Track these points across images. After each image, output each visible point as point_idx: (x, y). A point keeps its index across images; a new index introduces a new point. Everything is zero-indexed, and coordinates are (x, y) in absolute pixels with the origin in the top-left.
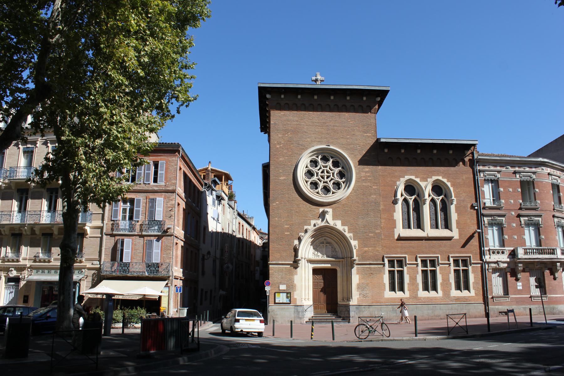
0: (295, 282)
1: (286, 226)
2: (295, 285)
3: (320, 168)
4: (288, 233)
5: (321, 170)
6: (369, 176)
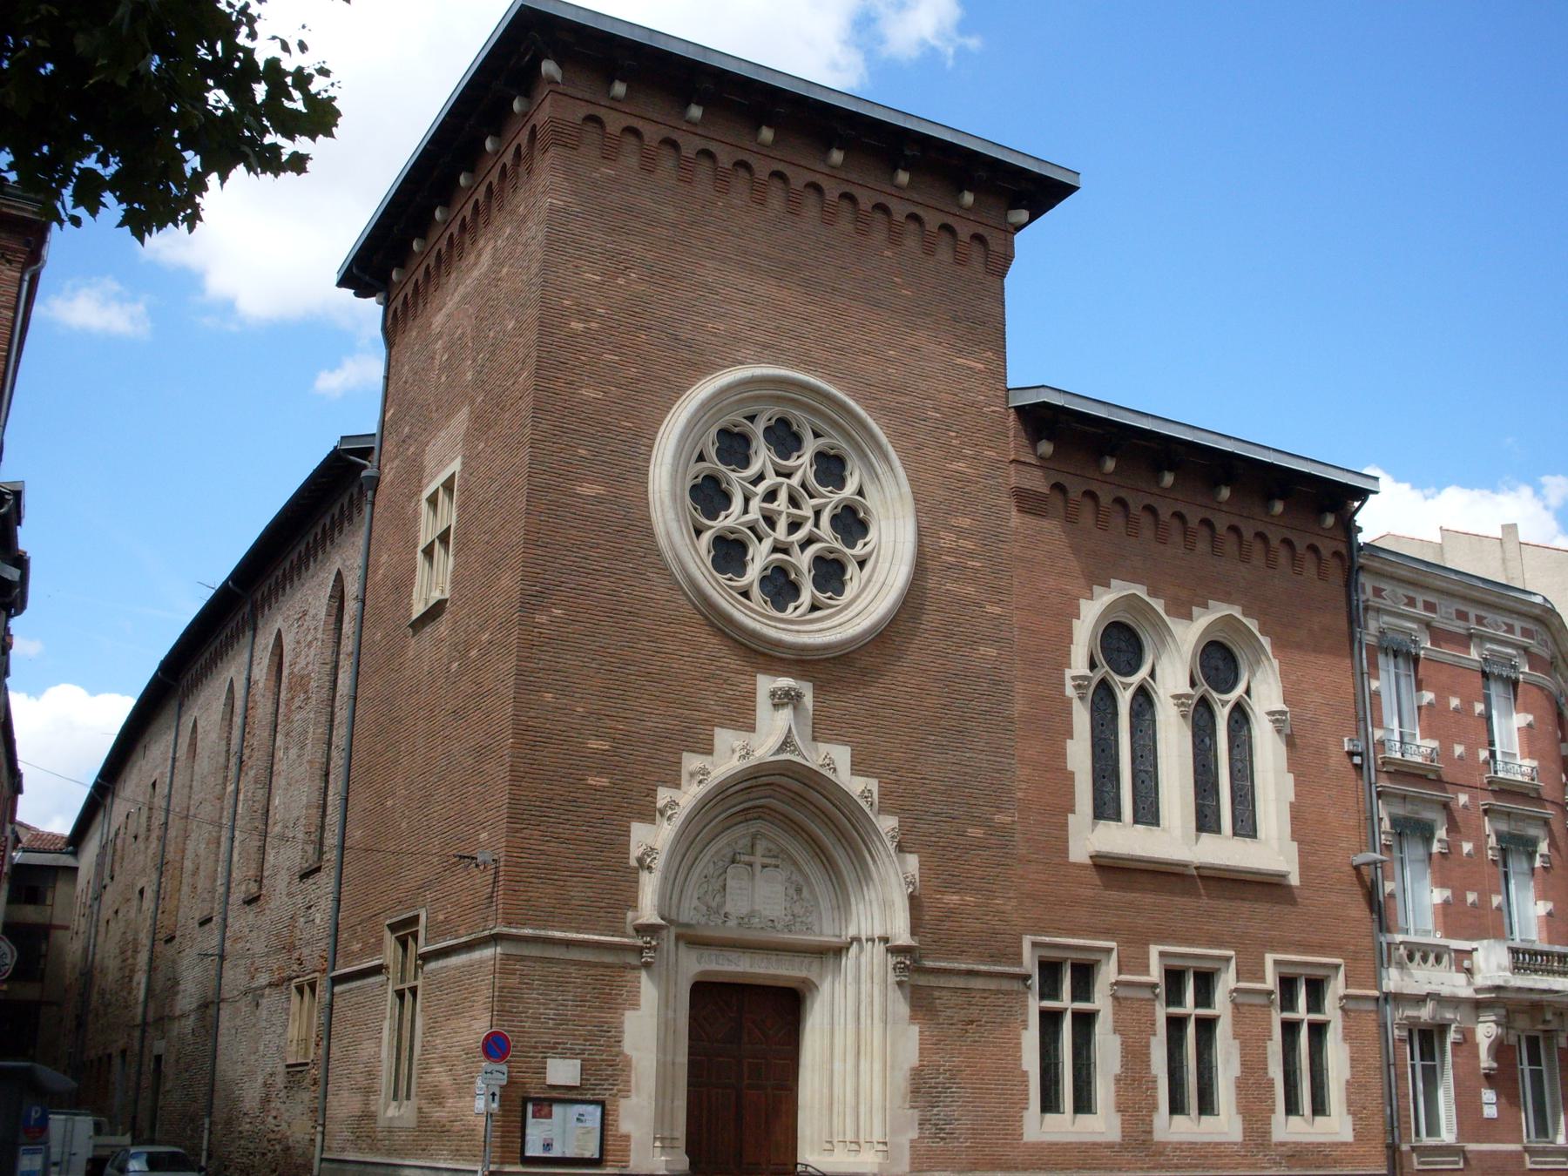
0: (628, 1046)
1: (594, 744)
2: (628, 1063)
3: (761, 477)
4: (605, 781)
5: (761, 488)
6: (971, 554)
